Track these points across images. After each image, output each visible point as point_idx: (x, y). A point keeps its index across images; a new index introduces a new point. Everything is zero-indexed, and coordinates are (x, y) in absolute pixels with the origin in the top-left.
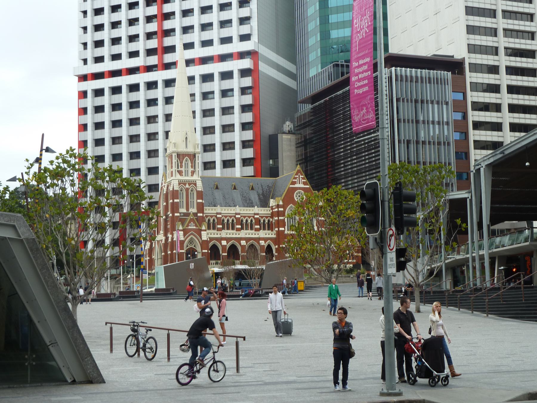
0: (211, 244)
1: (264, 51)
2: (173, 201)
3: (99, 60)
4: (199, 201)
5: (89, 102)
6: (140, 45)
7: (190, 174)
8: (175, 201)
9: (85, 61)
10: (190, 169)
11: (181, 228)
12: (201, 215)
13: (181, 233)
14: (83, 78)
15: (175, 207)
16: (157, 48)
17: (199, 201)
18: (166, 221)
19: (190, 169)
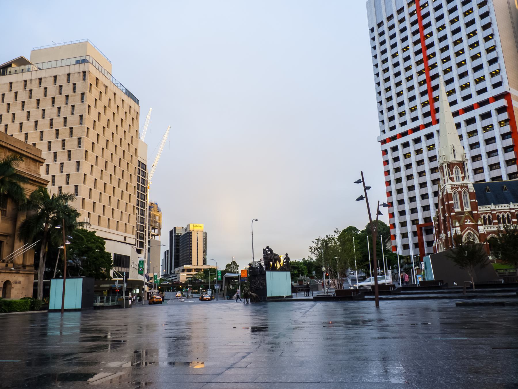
0: (489, 237)
1: (514, 92)
2: (448, 203)
3: (393, 128)
4: (472, 201)
5: (390, 156)
6: (419, 113)
7: (461, 179)
8: (450, 202)
9: (384, 132)
10: (461, 175)
11: (457, 224)
12: (476, 212)
13: (458, 229)
14: (384, 142)
15: (450, 208)
16: (430, 111)
17: (472, 201)
18: (444, 220)
19: (461, 175)
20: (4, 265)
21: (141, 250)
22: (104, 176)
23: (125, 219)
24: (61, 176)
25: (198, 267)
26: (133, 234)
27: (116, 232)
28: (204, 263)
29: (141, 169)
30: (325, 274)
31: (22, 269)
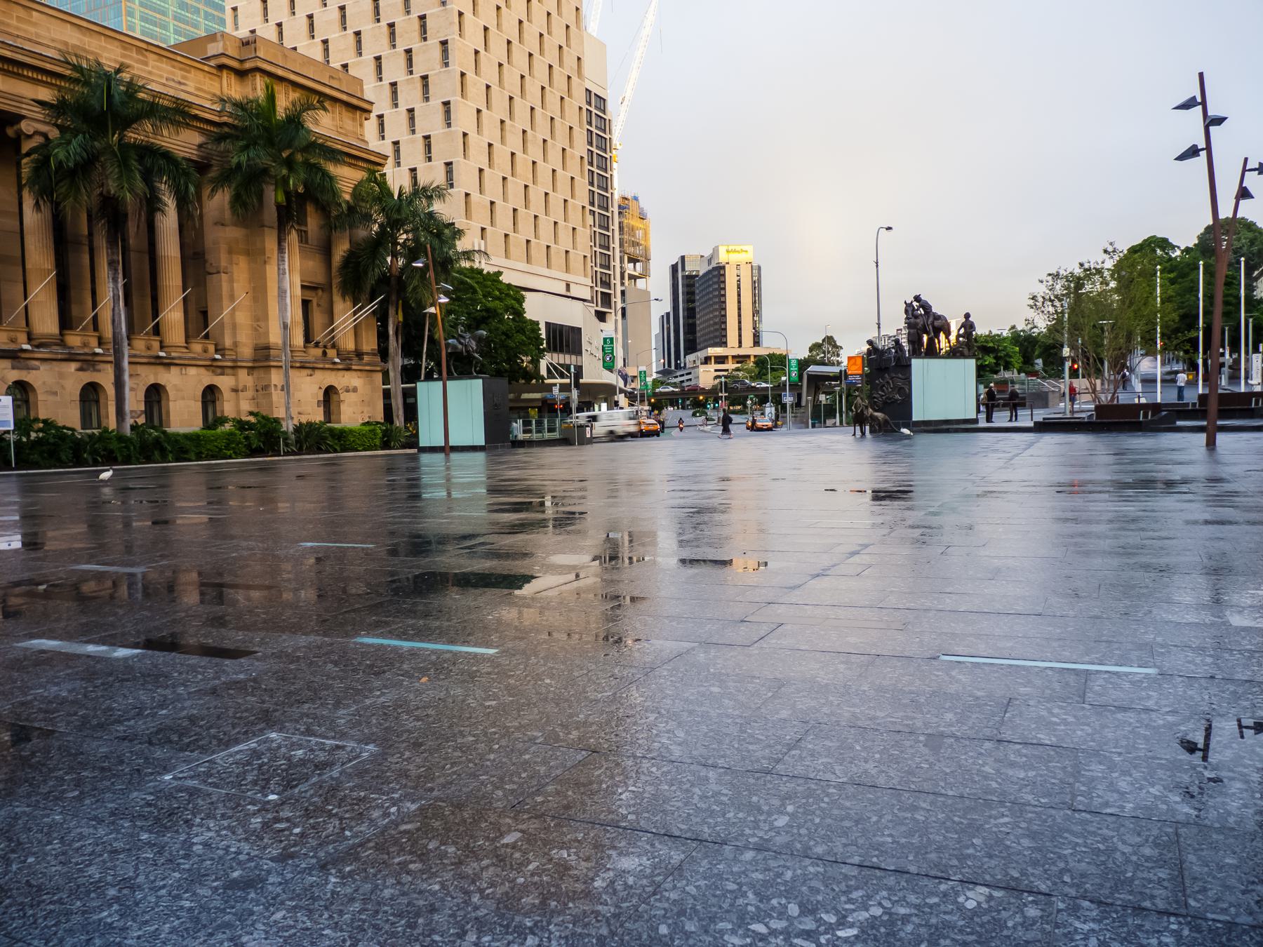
20: (319, 352)
21: (605, 313)
22: (508, 135)
23: (565, 241)
24: (413, 141)
25: (742, 352)
26: (585, 276)
27: (546, 272)
28: (757, 343)
29: (594, 111)
30: (1068, 364)
31: (356, 359)
